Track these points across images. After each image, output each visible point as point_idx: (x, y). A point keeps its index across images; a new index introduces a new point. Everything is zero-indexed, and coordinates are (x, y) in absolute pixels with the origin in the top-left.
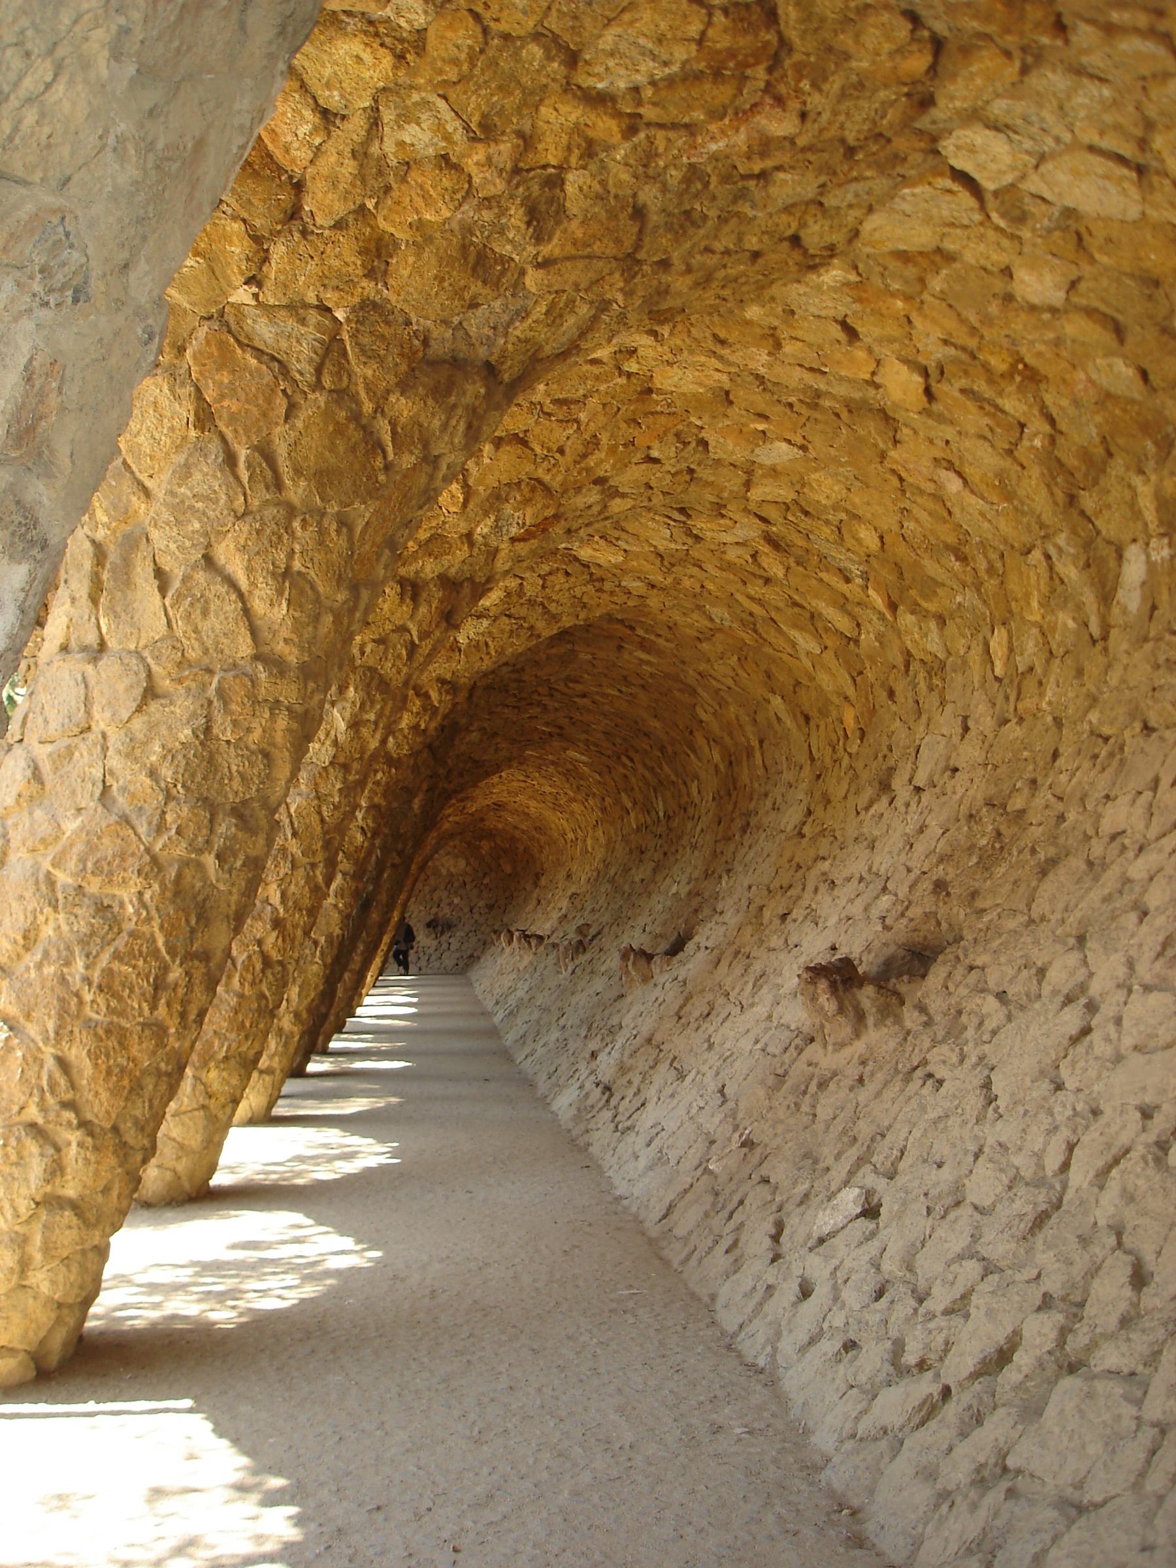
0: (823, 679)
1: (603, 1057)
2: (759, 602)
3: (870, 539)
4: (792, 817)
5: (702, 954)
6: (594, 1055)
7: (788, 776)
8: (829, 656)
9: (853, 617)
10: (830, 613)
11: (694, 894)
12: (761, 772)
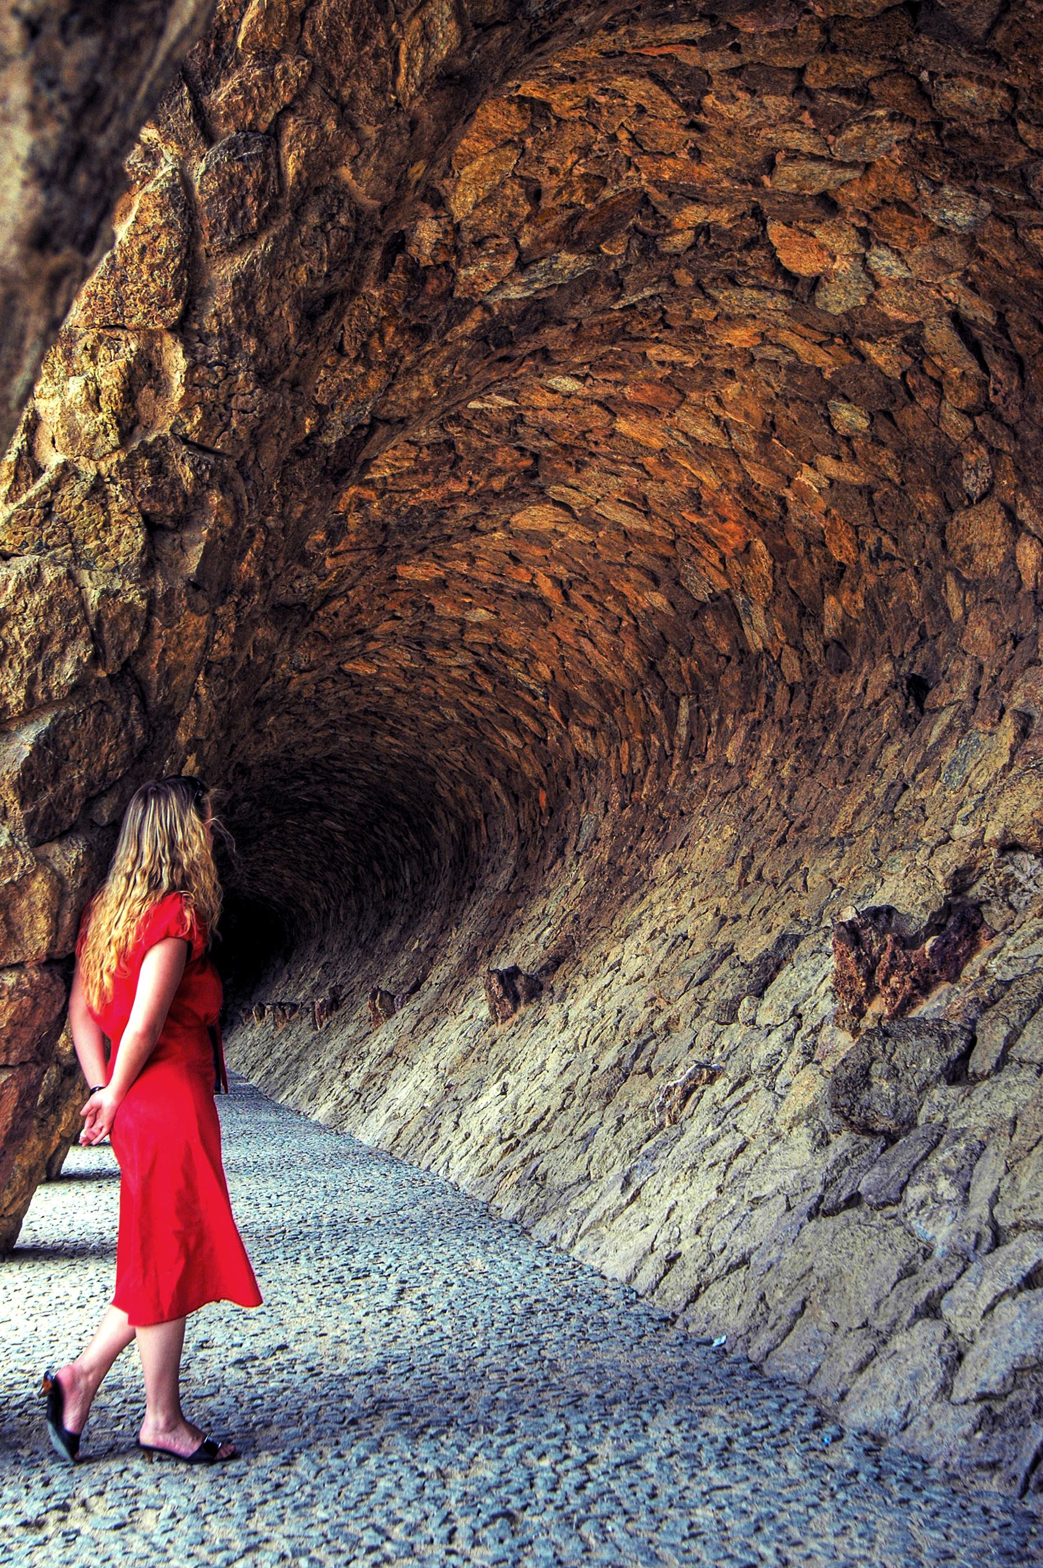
0: (525, 765)
1: (354, 1075)
2: (478, 707)
3: (545, 672)
4: (505, 875)
5: (432, 990)
6: (347, 1075)
7: (503, 845)
8: (527, 750)
9: (542, 724)
10: (526, 719)
11: (432, 946)
12: (484, 841)
